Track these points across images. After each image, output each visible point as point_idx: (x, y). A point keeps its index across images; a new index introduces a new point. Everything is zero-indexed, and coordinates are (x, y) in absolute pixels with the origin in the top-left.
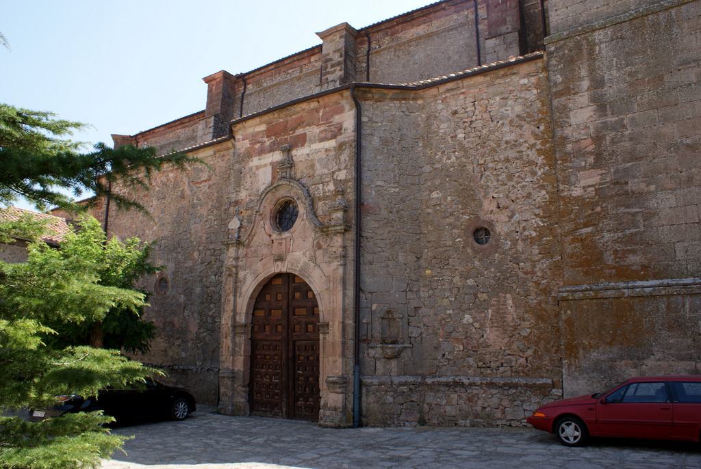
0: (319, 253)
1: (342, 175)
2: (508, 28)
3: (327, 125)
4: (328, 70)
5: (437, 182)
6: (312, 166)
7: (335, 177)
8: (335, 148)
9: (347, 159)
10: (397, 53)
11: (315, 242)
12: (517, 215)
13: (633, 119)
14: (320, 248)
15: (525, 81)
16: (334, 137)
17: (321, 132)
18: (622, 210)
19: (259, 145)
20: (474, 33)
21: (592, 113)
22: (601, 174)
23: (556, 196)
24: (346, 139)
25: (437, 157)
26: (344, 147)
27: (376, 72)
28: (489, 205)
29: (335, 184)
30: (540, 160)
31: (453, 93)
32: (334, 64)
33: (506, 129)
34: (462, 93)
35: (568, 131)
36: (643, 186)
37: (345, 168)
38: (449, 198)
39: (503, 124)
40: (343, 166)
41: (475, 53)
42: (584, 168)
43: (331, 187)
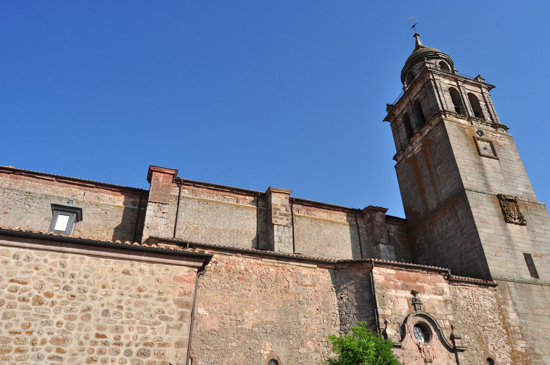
0: (451, 361)
1: (451, 318)
2: (384, 241)
3: (435, 286)
4: (276, 215)
5: (466, 330)
6: (433, 308)
7: (448, 318)
8: (443, 301)
9: (451, 309)
10: (313, 223)
11: (447, 354)
12: (502, 355)
13: (529, 323)
14: (451, 358)
15: (490, 293)
16: (441, 294)
17: (433, 289)
18: (536, 360)
19: (393, 282)
20: (357, 233)
21: (516, 316)
22: (525, 343)
23: (513, 351)
24: (448, 299)
25: (462, 317)
26: (448, 302)
27: (298, 229)
28: (491, 348)
29: (449, 322)
30: (504, 331)
31: (463, 287)
32: (282, 214)
33: (488, 312)
34: (467, 289)
35: (510, 321)
36: (539, 352)
37: (451, 315)
38: (473, 340)
39: (486, 310)
40: (450, 313)
41: (358, 244)
42: (519, 339)
43: (447, 323)
